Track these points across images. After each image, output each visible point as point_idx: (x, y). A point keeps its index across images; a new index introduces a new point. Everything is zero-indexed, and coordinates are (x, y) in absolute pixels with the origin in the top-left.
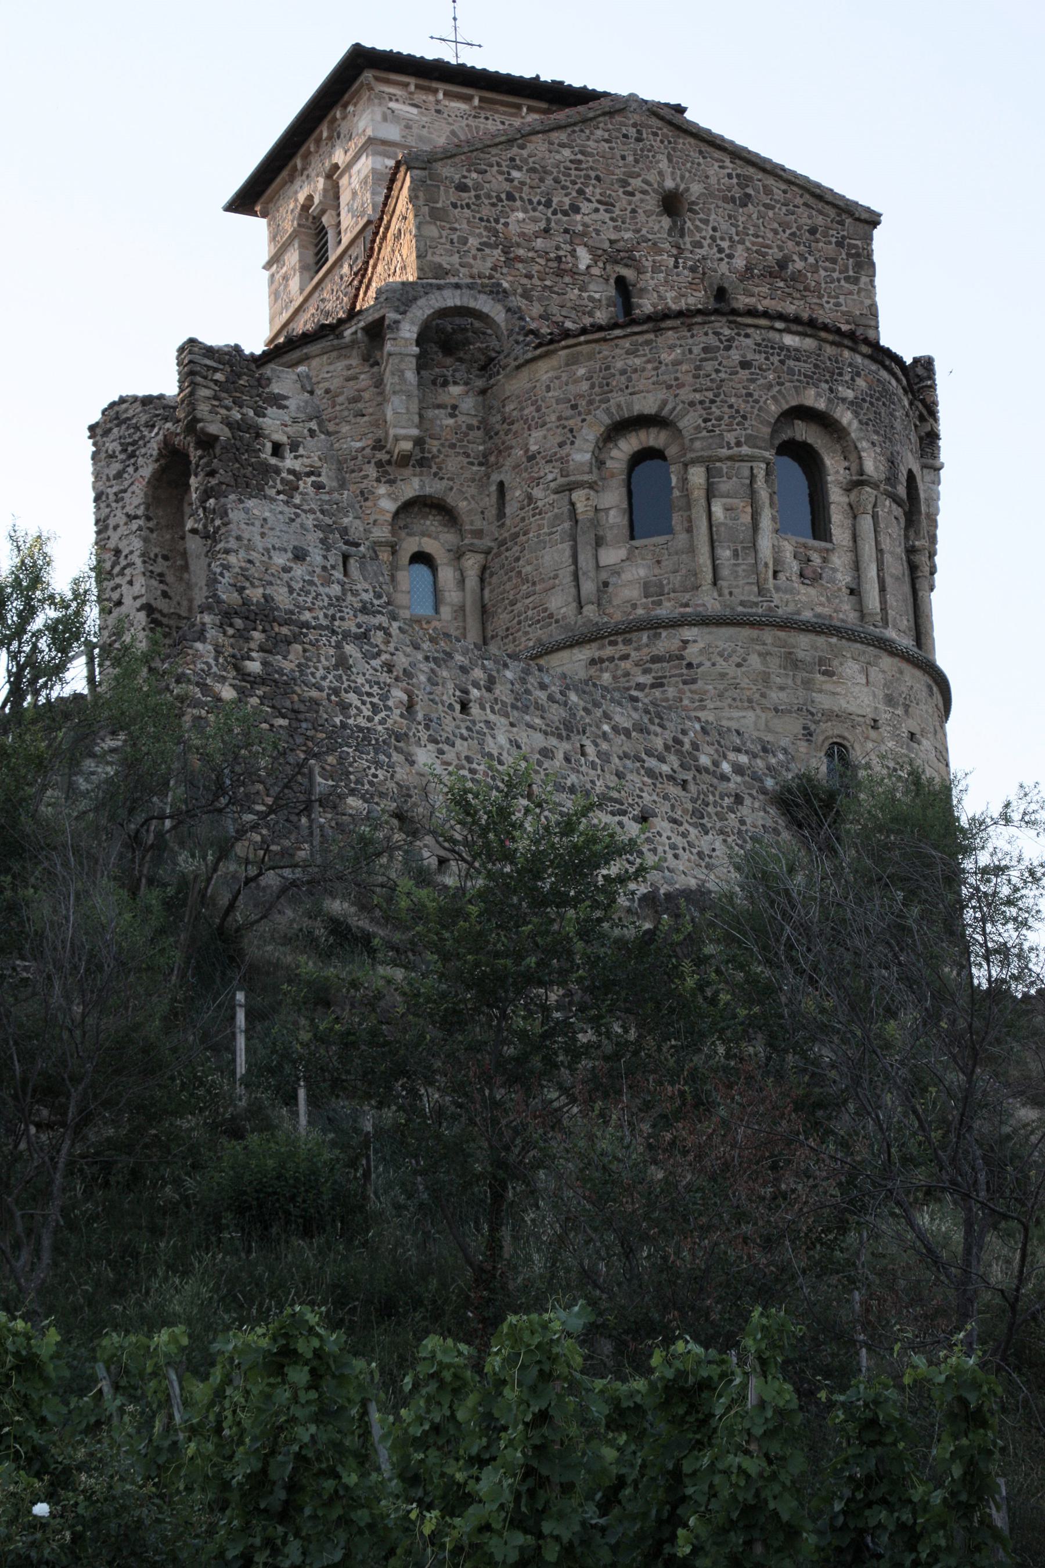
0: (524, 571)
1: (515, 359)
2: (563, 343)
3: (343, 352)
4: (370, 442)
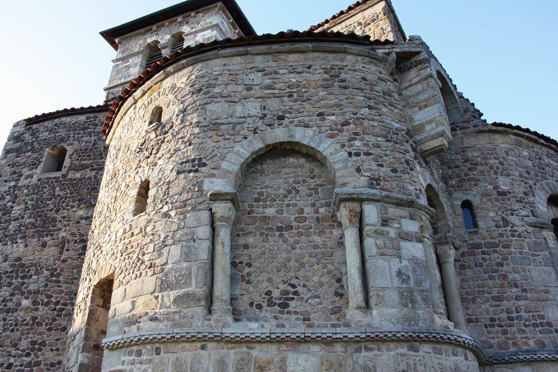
0: (510, 276)
1: (474, 126)
2: (516, 131)
3: (374, 61)
4: (405, 128)
